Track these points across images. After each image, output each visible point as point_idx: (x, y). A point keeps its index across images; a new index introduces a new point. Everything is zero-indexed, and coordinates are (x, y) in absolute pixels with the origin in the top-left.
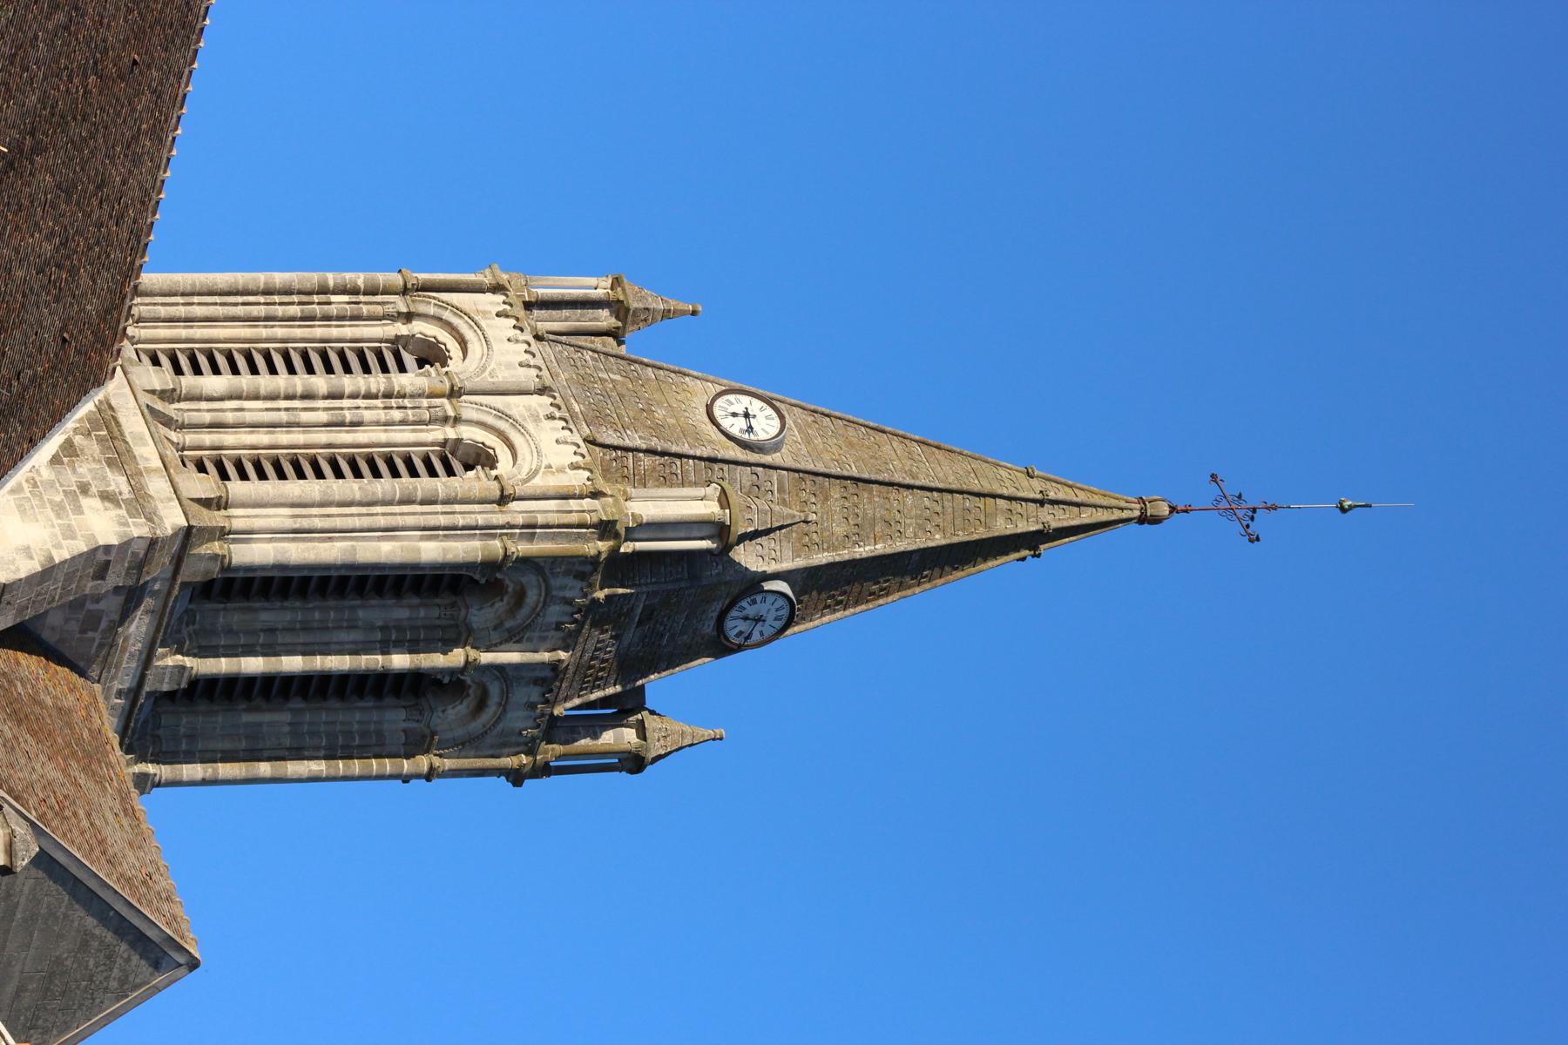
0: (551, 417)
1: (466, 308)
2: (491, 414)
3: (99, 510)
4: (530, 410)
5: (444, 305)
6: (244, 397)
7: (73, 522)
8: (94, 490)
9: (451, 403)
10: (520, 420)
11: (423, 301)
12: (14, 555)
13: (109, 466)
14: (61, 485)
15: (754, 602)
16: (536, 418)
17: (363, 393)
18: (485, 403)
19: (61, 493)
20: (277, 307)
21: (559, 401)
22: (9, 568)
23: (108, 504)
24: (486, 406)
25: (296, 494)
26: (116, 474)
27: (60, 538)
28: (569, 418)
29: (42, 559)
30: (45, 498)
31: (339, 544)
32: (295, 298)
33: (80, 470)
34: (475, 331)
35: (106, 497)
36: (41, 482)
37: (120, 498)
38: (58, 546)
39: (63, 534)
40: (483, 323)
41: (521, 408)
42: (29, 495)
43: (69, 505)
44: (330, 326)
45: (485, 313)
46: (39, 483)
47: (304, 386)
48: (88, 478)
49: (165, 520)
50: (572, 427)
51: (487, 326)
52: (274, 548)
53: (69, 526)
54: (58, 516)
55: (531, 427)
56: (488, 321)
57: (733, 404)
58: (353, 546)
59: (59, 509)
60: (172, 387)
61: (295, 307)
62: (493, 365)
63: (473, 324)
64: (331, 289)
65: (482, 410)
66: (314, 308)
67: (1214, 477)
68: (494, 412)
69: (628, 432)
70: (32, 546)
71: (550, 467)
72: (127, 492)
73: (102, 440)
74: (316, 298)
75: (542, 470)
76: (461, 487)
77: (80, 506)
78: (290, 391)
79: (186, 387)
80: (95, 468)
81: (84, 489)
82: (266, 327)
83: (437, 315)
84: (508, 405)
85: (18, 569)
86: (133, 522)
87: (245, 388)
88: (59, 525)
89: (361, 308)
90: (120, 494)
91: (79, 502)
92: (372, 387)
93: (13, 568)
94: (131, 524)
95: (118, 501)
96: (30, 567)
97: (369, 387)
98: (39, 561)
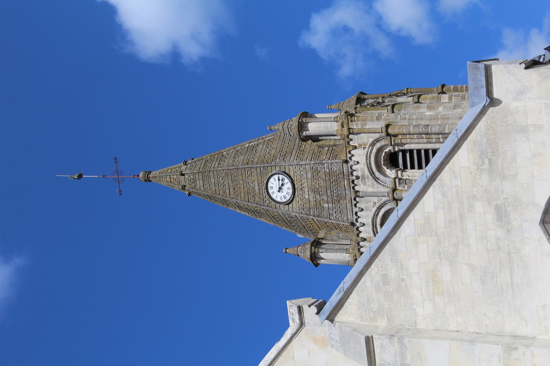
0: (358, 178)
9: (396, 187)
16: (363, 176)
21: (352, 185)
24: (382, 184)
28: (350, 175)
34: (376, 231)
41: (368, 184)
50: (350, 170)
51: (369, 233)
55: (367, 172)
57: (284, 196)
58: (454, 109)
62: (374, 210)
67: (121, 194)
68: (379, 181)
69: (328, 171)
75: (367, 147)
76: (403, 129)
84: (373, 186)
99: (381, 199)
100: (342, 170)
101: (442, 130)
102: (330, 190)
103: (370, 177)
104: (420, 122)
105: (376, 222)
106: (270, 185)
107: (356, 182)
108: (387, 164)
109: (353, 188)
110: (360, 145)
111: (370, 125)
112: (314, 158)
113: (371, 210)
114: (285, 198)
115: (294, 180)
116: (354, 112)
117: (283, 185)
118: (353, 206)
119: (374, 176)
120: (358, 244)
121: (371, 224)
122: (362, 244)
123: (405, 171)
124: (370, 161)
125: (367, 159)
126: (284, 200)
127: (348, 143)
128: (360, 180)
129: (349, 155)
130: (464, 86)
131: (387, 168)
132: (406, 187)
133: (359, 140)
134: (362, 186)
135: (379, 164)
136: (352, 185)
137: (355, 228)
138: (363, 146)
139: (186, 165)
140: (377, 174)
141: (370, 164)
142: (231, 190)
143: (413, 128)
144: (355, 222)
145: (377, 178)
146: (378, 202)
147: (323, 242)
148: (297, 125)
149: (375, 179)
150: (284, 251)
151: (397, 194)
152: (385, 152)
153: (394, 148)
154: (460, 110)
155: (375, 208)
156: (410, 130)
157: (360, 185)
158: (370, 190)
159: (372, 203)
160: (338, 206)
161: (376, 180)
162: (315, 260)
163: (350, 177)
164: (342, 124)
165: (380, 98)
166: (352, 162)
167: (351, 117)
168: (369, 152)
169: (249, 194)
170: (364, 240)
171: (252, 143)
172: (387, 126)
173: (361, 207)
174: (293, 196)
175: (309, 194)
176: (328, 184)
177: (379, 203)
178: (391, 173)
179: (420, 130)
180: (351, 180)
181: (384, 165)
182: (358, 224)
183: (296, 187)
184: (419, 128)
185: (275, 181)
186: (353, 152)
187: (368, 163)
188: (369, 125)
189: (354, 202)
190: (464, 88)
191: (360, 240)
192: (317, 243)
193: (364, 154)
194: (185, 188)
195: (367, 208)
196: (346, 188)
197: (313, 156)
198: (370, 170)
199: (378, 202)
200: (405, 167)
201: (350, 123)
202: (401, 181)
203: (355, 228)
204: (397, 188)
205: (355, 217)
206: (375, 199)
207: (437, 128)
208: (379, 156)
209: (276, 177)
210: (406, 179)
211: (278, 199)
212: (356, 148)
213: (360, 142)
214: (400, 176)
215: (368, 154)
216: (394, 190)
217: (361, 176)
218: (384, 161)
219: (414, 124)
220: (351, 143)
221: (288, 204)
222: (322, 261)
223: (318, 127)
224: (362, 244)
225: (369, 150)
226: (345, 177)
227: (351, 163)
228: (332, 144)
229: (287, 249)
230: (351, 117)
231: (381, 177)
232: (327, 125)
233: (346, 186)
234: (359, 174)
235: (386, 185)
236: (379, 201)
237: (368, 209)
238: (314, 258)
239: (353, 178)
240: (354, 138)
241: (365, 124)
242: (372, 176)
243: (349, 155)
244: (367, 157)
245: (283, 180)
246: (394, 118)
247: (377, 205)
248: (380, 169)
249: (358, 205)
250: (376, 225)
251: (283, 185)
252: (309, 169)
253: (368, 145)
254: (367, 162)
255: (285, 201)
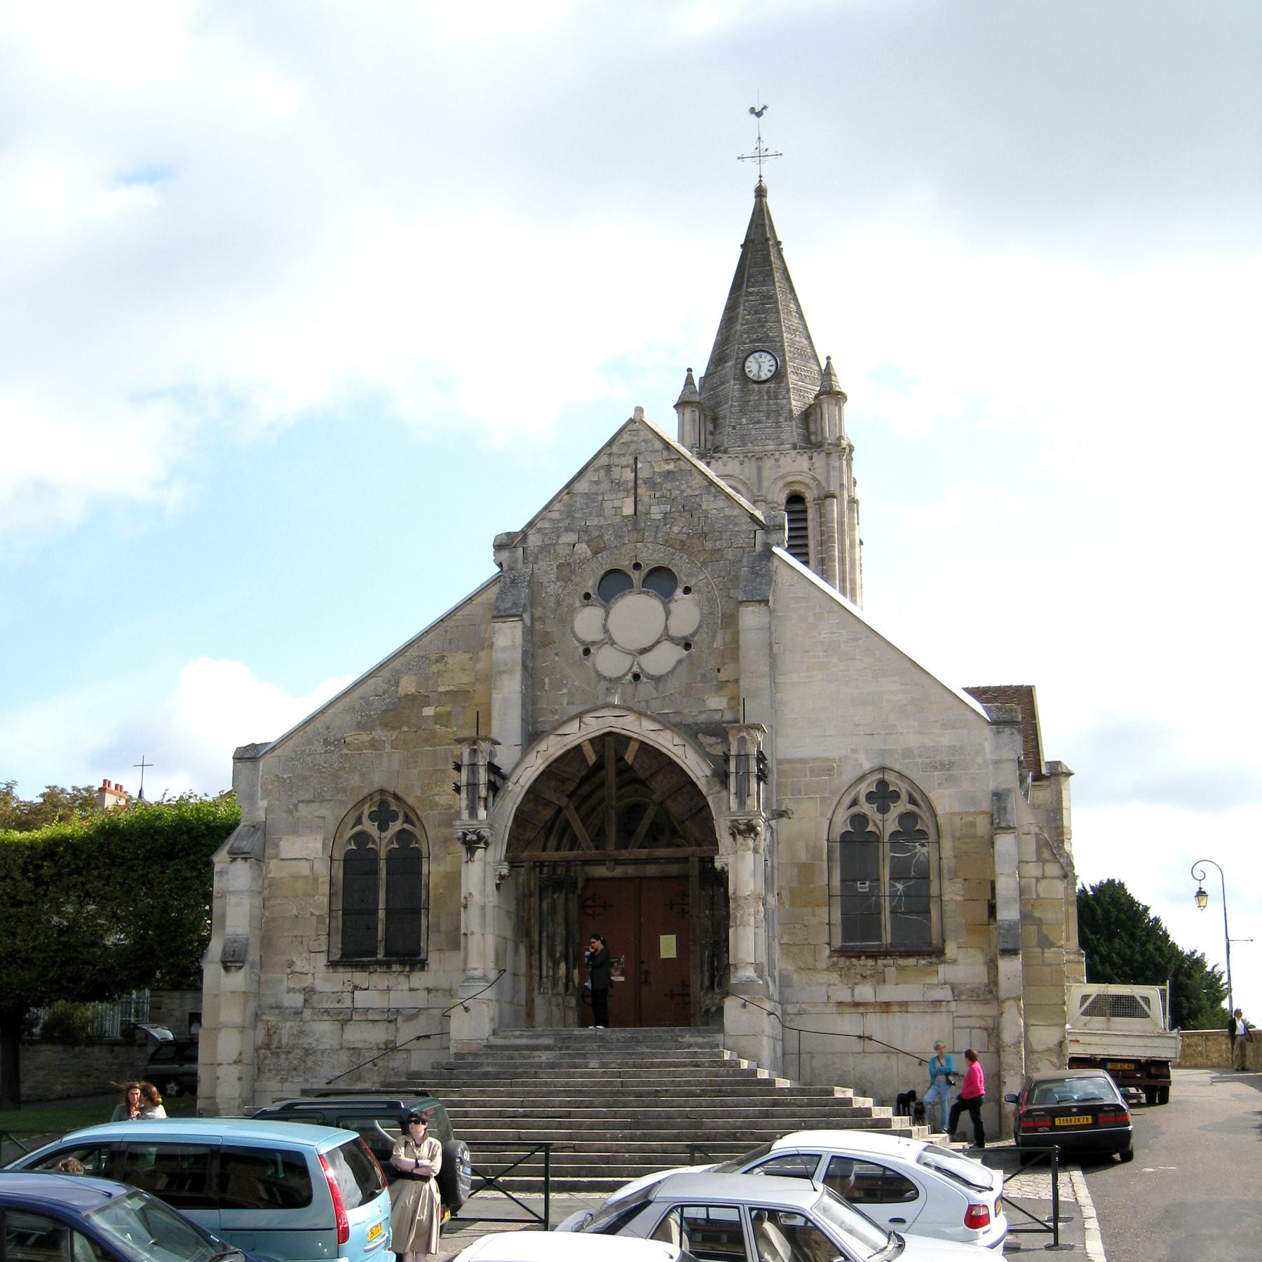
0: (777, 460)
16: (778, 467)
21: (769, 454)
55: (783, 471)
62: (742, 477)
67: (739, 158)
103: (777, 476)
106: (764, 354)
113: (741, 474)
126: (747, 370)
140: (781, 483)
155: (744, 480)
178: (782, 498)
200: (789, 513)
206: (754, 480)
211: (747, 364)
212: (811, 458)
213: (817, 465)
220: (815, 454)
234: (782, 461)
243: (802, 451)
249: (746, 459)
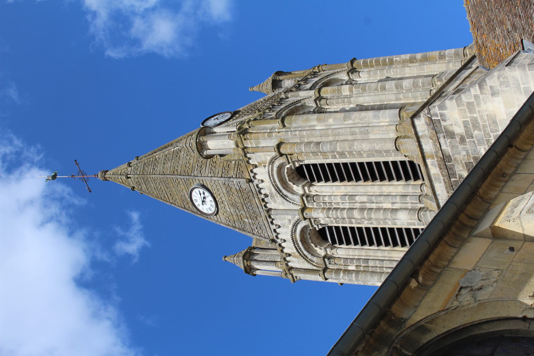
0: (266, 195)
1: (302, 260)
2: (289, 198)
3: (455, 125)
4: (274, 200)
5: (310, 261)
6: (390, 210)
7: (468, 115)
8: (458, 139)
9: (305, 205)
10: (278, 195)
11: (319, 264)
12: (500, 89)
13: (450, 156)
14: (474, 142)
15: (215, 123)
16: (271, 194)
17: (339, 210)
18: (291, 204)
19: (474, 136)
20: (379, 266)
21: (263, 204)
22: (504, 78)
23: (451, 129)
24: (291, 202)
25: (364, 144)
26: (446, 150)
27: (475, 103)
29: (485, 87)
30: (482, 133)
31: (351, 122)
32: (370, 269)
33: (464, 153)
34: (298, 247)
35: (451, 135)
36: (484, 144)
37: (445, 134)
38: (476, 97)
39: (474, 106)
40: (295, 250)
41: (278, 201)
42: (492, 134)
43: (470, 128)
44: (359, 256)
45: (295, 257)
46: (486, 143)
47: (363, 214)
48: (460, 147)
49: (424, 123)
50: (257, 189)
51: (292, 249)
52: (379, 118)
53: (471, 112)
54: (476, 119)
56: (293, 251)
57: (209, 208)
58: (345, 121)
59: (476, 125)
60: (422, 213)
61: (371, 265)
62: (291, 226)
63: (299, 251)
64: (354, 272)
65: (293, 200)
66: (363, 264)
67: (90, 191)
68: (288, 199)
69: (238, 188)
70: (490, 96)
71: (265, 166)
72: (441, 138)
73: (453, 174)
74: (362, 269)
75: (267, 165)
76: (295, 149)
77: (465, 127)
78: (369, 211)
79: (415, 214)
80: (457, 155)
81: (463, 140)
82: (385, 257)
83: (313, 257)
84: (283, 203)
85: (498, 78)
86: (438, 117)
87: (389, 213)
88: (475, 112)
89: (344, 262)
90: (444, 137)
91: (465, 130)
92: (335, 212)
93: (501, 79)
94: (439, 115)
95: (446, 132)
96: (492, 80)
97: (336, 212)
98: (487, 85)
99: (295, 217)
100: (250, 189)
101: (334, 150)
102: (245, 206)
104: (311, 139)
105: (296, 238)
106: (194, 198)
107: (266, 199)
108: (293, 178)
109: (265, 206)
110: (260, 164)
111: (263, 144)
112: (225, 172)
113: (288, 227)
114: (211, 210)
115: (213, 193)
116: (248, 127)
117: (204, 198)
118: (270, 224)
119: (281, 194)
120: (285, 259)
121: (291, 239)
122: (288, 259)
123: (313, 185)
124: (274, 179)
125: (270, 177)
126: (210, 212)
127: (248, 162)
128: (269, 197)
129: (252, 175)
130: (374, 61)
131: (294, 184)
132: (315, 205)
133: (258, 158)
134: (273, 203)
135: (284, 180)
136: (263, 204)
137: (277, 244)
138: (263, 164)
139: (130, 167)
140: (284, 191)
141: (275, 182)
142: (169, 195)
143: (304, 148)
144: (275, 238)
145: (285, 196)
146: (293, 220)
147: (255, 252)
148: (196, 146)
149: (283, 197)
150: (224, 260)
151: (307, 214)
152: (287, 168)
153: (294, 164)
154: (351, 122)
156: (301, 150)
157: (270, 203)
158: (282, 207)
159: (287, 220)
160: (257, 222)
161: (284, 198)
162: (251, 271)
163: (259, 196)
164: (236, 144)
165: (283, 93)
166: (256, 181)
167: (244, 135)
168: (270, 170)
169: (183, 201)
170: (290, 255)
171: (176, 148)
172: (279, 146)
173: (278, 224)
174: (216, 208)
175: (229, 208)
176: (242, 200)
177: (293, 221)
178: (298, 189)
179: (312, 149)
180: (261, 199)
181: (290, 181)
182: (279, 241)
183: (217, 199)
184: (311, 148)
185: (198, 194)
186: (255, 170)
187: (272, 181)
188: (262, 143)
189: (270, 220)
190: (374, 62)
191: (285, 256)
192: (249, 255)
193: (266, 173)
194: (135, 189)
195: (284, 226)
196: (258, 206)
197: (223, 171)
198: (276, 188)
199: (293, 220)
200: (312, 180)
201: (244, 141)
202: (309, 199)
203: (277, 244)
204: (307, 205)
205: (275, 234)
206: (290, 217)
207: (328, 147)
208: (282, 172)
209: (196, 190)
210: (314, 195)
212: (256, 166)
213: (259, 161)
214: (307, 191)
215: (270, 172)
216: (303, 210)
217: (270, 194)
218: (288, 176)
219: (306, 141)
220: (250, 161)
221: (216, 215)
222: (258, 272)
223: (217, 146)
224: (288, 259)
225: (270, 168)
226: (254, 195)
227: (256, 182)
228: (236, 159)
229: (225, 257)
230: (244, 135)
231: (289, 195)
232: (224, 143)
233: (257, 204)
234: (268, 192)
235: (295, 203)
236: (293, 218)
237: (285, 226)
238: (249, 270)
239: (262, 197)
240: (252, 157)
241: (259, 143)
242: (280, 194)
244: (270, 175)
245: (204, 193)
246: (285, 135)
247: (292, 222)
248: (286, 185)
250: (297, 241)
251: (204, 198)
252: (222, 184)
253: (267, 163)
254: (271, 180)
255: (212, 213)
